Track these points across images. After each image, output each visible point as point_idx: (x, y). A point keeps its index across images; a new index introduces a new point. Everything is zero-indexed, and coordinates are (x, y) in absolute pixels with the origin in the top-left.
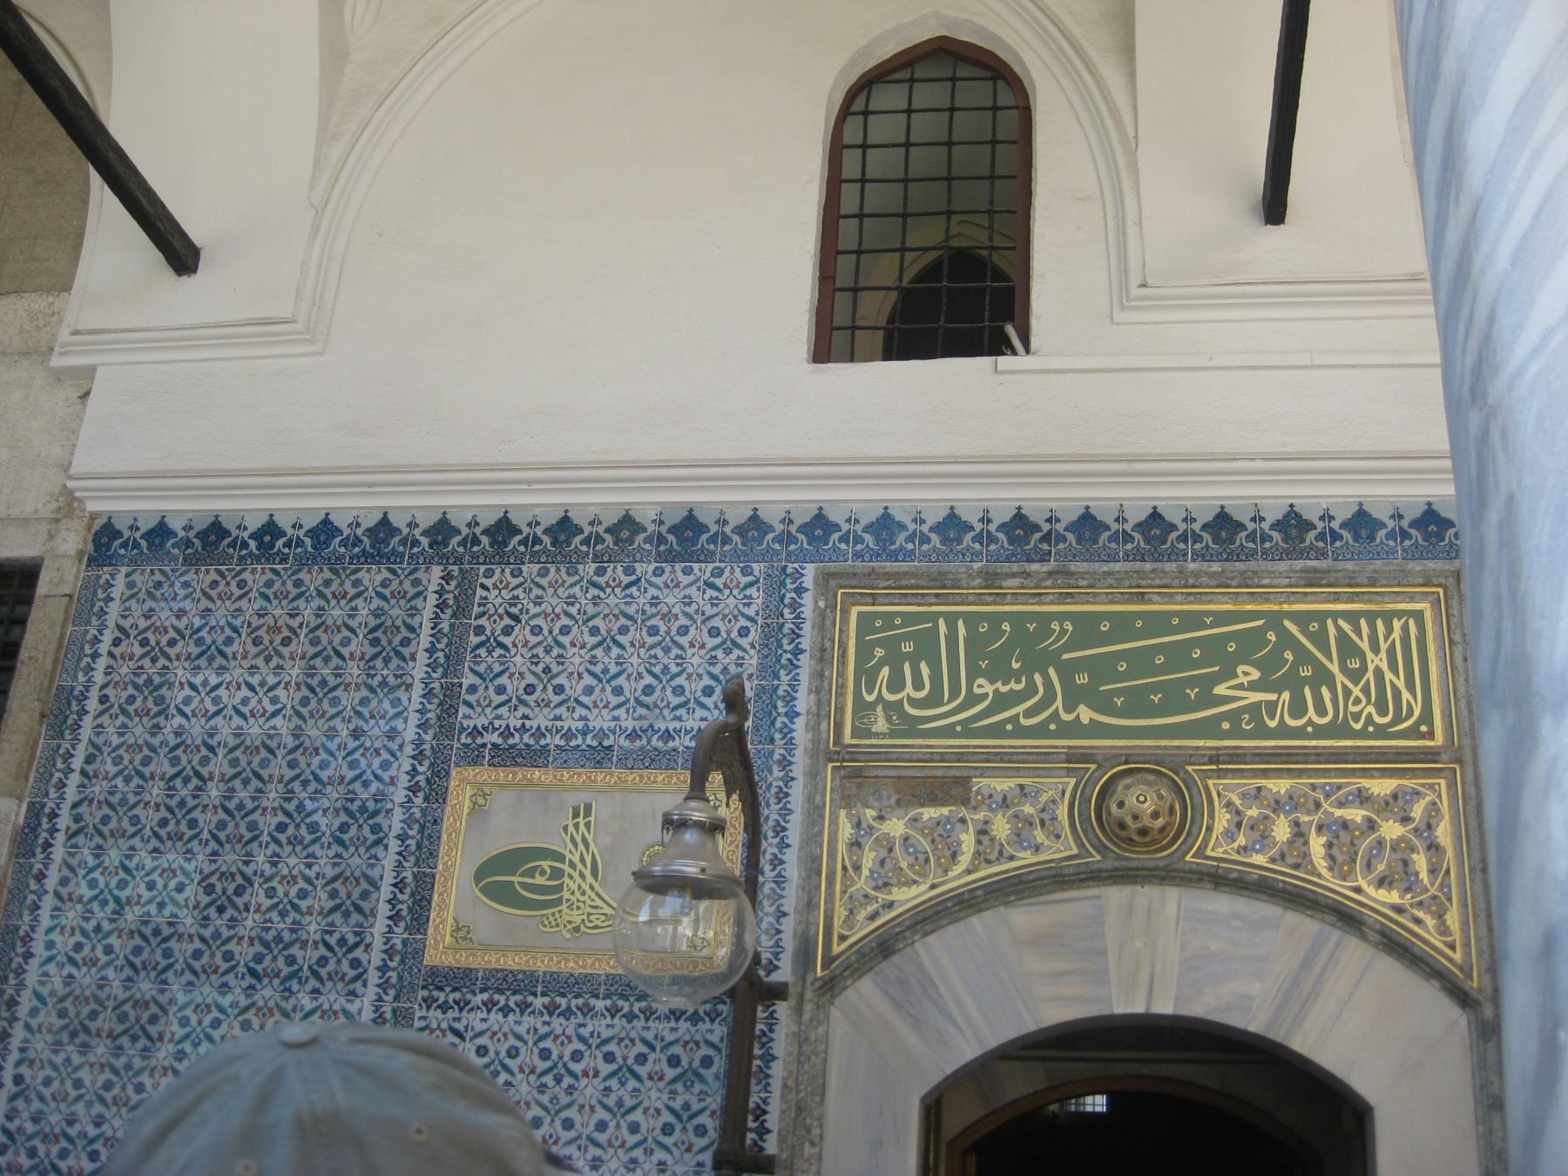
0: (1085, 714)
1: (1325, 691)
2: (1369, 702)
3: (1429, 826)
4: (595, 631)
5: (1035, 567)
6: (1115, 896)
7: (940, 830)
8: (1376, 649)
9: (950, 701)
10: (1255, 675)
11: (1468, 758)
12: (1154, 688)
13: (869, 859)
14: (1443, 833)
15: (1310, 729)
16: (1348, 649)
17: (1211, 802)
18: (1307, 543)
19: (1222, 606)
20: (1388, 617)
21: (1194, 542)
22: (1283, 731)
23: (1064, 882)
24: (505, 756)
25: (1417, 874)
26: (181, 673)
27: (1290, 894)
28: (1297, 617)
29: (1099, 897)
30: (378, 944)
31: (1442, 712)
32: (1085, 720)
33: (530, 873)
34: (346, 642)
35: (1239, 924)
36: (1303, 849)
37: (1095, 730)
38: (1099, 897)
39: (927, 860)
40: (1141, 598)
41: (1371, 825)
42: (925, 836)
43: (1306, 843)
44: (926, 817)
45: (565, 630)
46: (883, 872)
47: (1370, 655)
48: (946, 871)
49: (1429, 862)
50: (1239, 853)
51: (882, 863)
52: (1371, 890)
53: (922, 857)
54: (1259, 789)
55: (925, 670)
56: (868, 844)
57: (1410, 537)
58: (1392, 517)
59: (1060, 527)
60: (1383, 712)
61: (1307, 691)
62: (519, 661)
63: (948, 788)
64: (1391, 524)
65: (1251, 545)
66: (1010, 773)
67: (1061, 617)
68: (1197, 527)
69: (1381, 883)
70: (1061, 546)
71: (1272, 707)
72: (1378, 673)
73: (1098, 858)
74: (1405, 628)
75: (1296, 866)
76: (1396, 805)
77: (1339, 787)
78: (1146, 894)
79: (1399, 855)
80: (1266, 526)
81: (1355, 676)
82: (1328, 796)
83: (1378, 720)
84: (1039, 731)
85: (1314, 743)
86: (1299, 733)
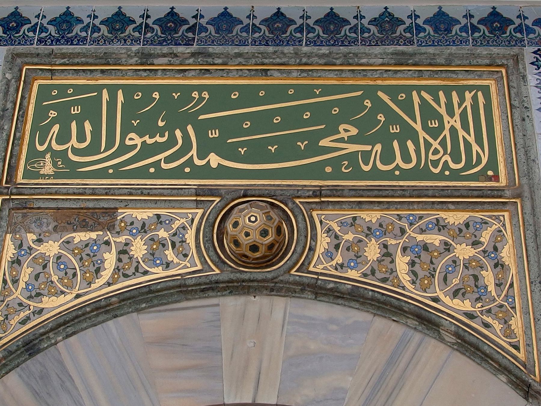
0: (214, 160)
1: (410, 144)
2: (445, 153)
3: (496, 249)
5: (181, 49)
6: (231, 304)
7: (87, 250)
8: (451, 113)
9: (105, 151)
10: (354, 131)
11: (527, 194)
13: (26, 273)
14: (507, 254)
15: (397, 173)
16: (429, 113)
17: (313, 227)
18: (398, 34)
19: (328, 80)
21: (308, 33)
22: (375, 174)
23: (187, 292)
25: (486, 287)
27: (378, 301)
28: (387, 89)
29: (218, 305)
31: (506, 160)
32: (214, 165)
35: (335, 327)
36: (390, 266)
37: (222, 172)
38: (218, 305)
39: (75, 275)
42: (75, 255)
43: (393, 262)
44: (77, 240)
46: (37, 284)
47: (446, 118)
48: (90, 284)
49: (496, 277)
50: (336, 269)
51: (37, 277)
52: (447, 300)
53: (70, 272)
54: (355, 219)
55: (88, 127)
56: (26, 262)
57: (479, 30)
58: (465, 16)
59: (203, 21)
60: (456, 159)
61: (396, 144)
63: (100, 217)
64: (463, 21)
65: (353, 35)
66: (149, 205)
67: (200, 88)
68: (311, 22)
69: (455, 294)
70: (203, 34)
71: (366, 156)
72: (453, 131)
73: (218, 271)
74: (475, 98)
75: (384, 280)
76: (468, 232)
77: (421, 218)
78: (257, 303)
79: (471, 272)
80: (365, 22)
81: (434, 133)
82: (411, 224)
83: (453, 166)
85: (401, 183)
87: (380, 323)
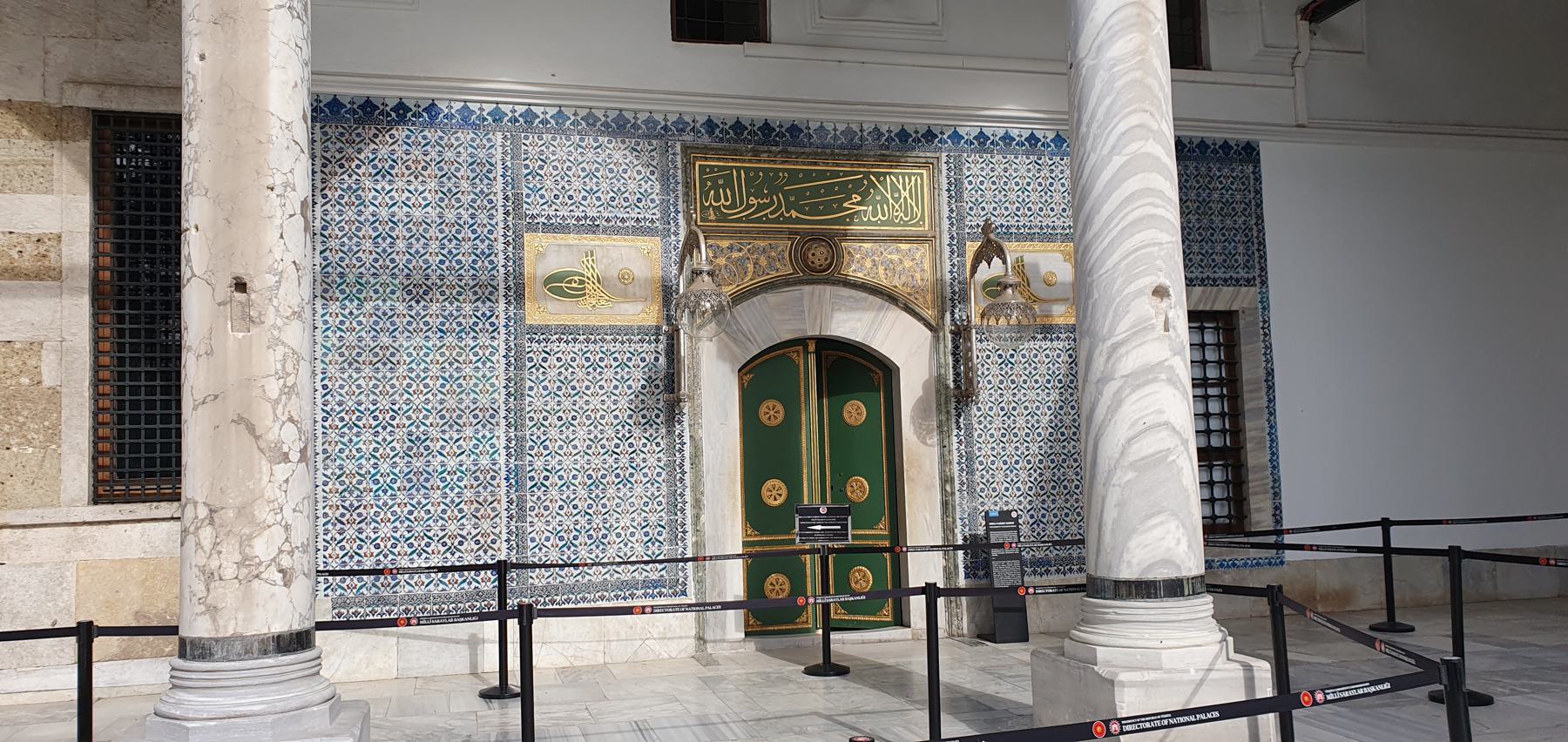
0: (794, 214)
4: (583, 170)
6: (807, 288)
12: (820, 203)
20: (910, 175)
22: (869, 223)
24: (549, 228)
26: (368, 183)
28: (874, 174)
30: (502, 315)
33: (570, 282)
34: (458, 170)
37: (798, 221)
40: (816, 164)
41: (901, 261)
45: (569, 169)
62: (549, 183)
67: (784, 170)
81: (896, 200)
84: (776, 221)
86: (875, 224)
87: (871, 297)
